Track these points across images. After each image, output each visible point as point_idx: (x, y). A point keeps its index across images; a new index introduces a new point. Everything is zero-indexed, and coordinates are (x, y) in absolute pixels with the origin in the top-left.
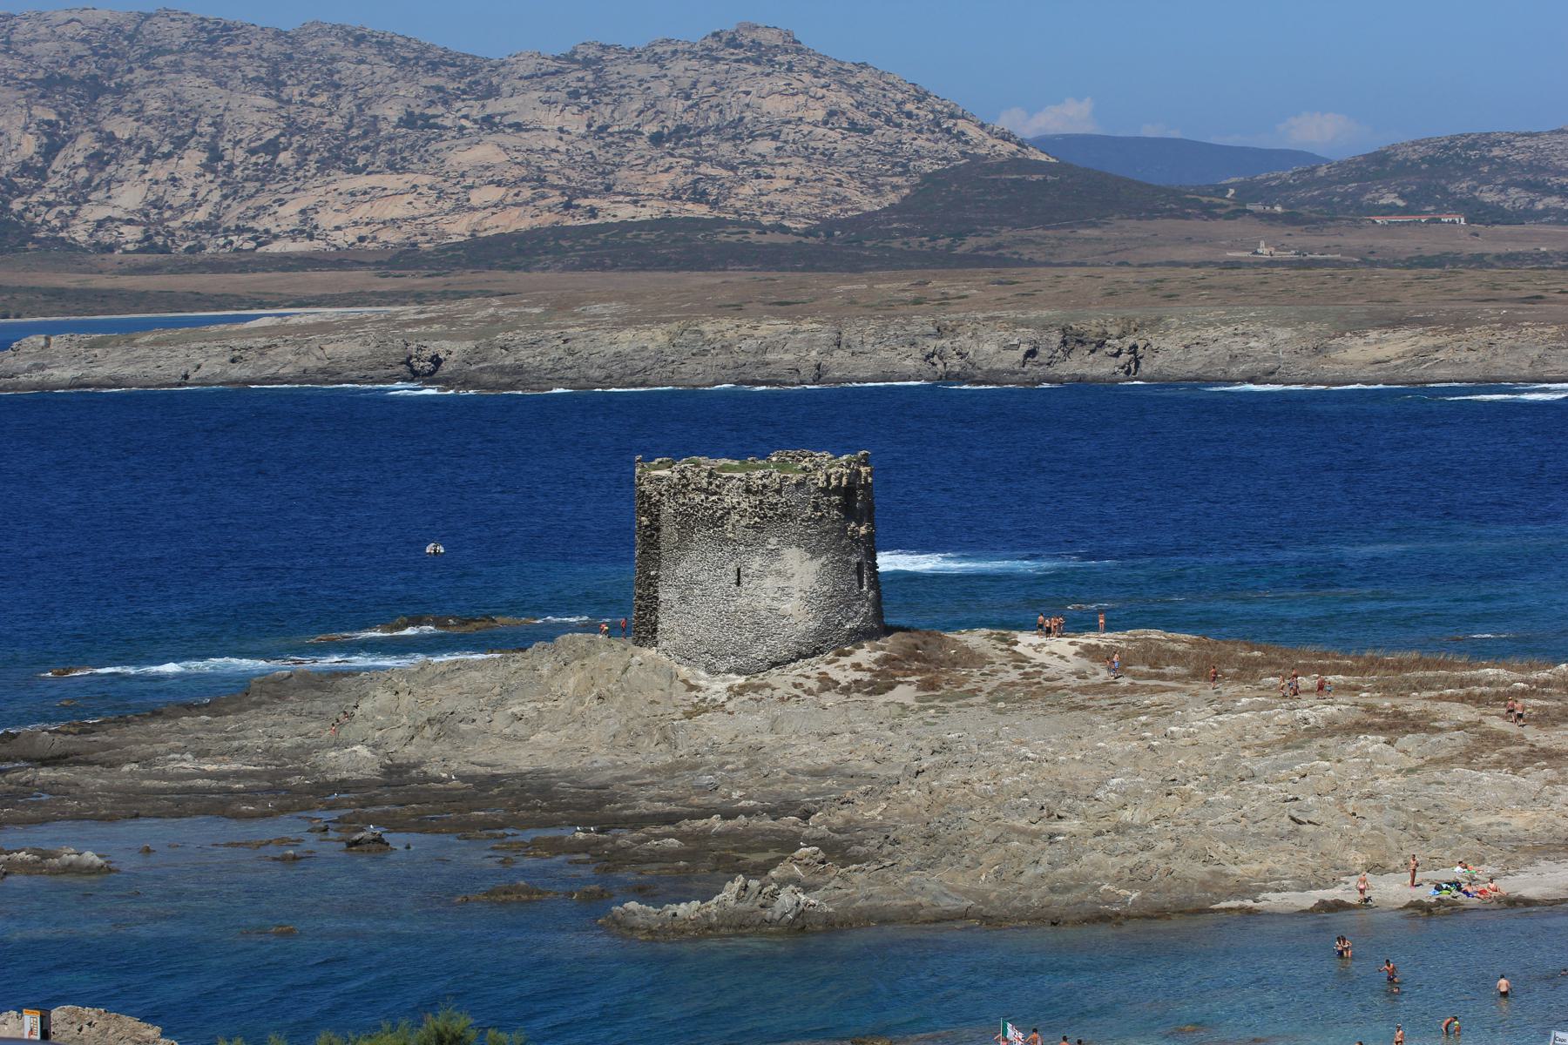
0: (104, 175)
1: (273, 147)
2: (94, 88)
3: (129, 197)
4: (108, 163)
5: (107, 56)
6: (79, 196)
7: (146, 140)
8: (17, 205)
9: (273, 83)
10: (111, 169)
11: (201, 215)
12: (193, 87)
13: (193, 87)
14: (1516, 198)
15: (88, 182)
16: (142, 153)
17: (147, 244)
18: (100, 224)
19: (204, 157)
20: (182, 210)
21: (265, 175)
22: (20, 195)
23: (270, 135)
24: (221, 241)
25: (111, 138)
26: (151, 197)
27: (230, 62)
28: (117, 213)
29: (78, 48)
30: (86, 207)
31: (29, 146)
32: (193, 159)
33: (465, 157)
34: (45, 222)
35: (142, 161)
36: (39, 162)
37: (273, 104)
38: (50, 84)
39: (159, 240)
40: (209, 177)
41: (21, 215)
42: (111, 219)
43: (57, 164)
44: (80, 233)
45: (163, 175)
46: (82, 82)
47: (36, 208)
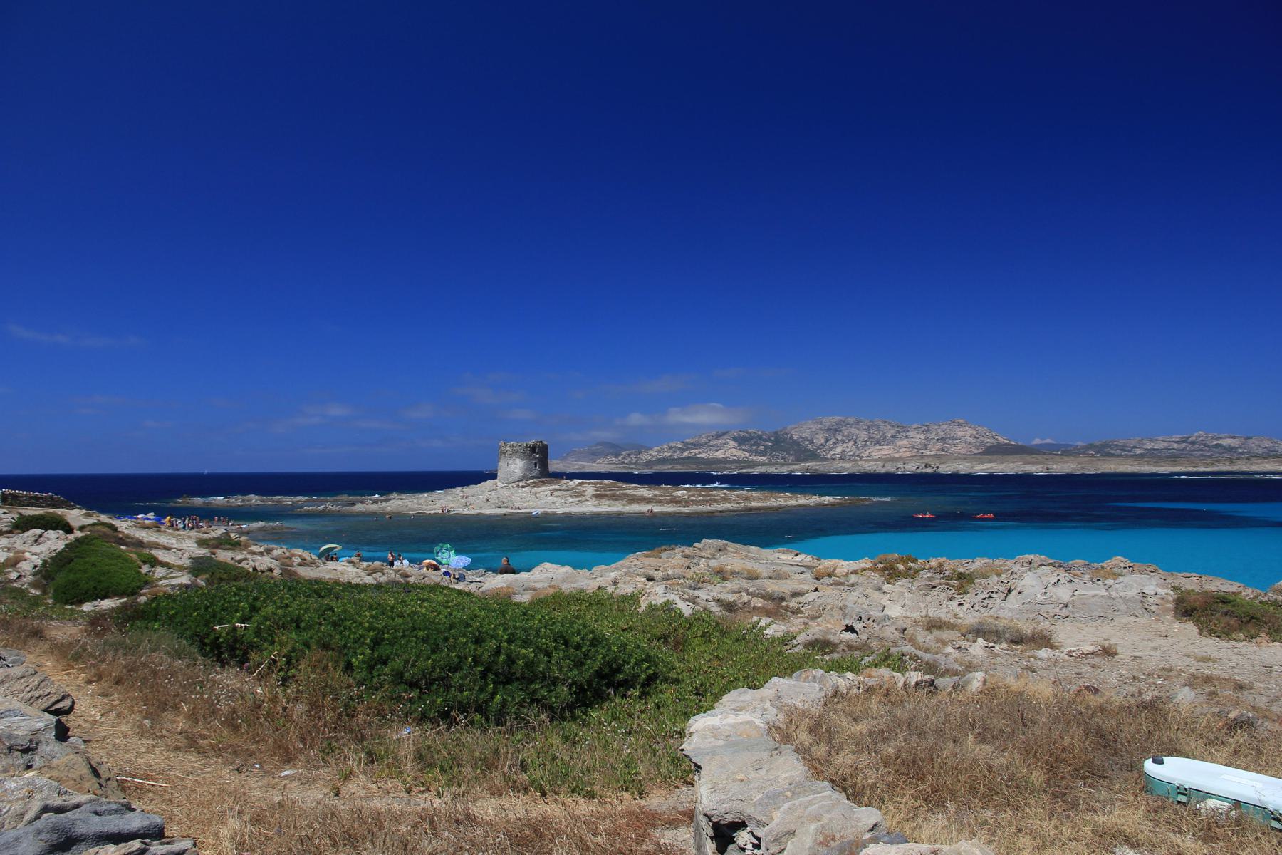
2: (836, 430)
3: (839, 450)
6: (830, 450)
9: (868, 430)
12: (853, 430)
13: (853, 430)
14: (1119, 452)
21: (864, 446)
33: (900, 443)
38: (828, 430)
47: (822, 452)
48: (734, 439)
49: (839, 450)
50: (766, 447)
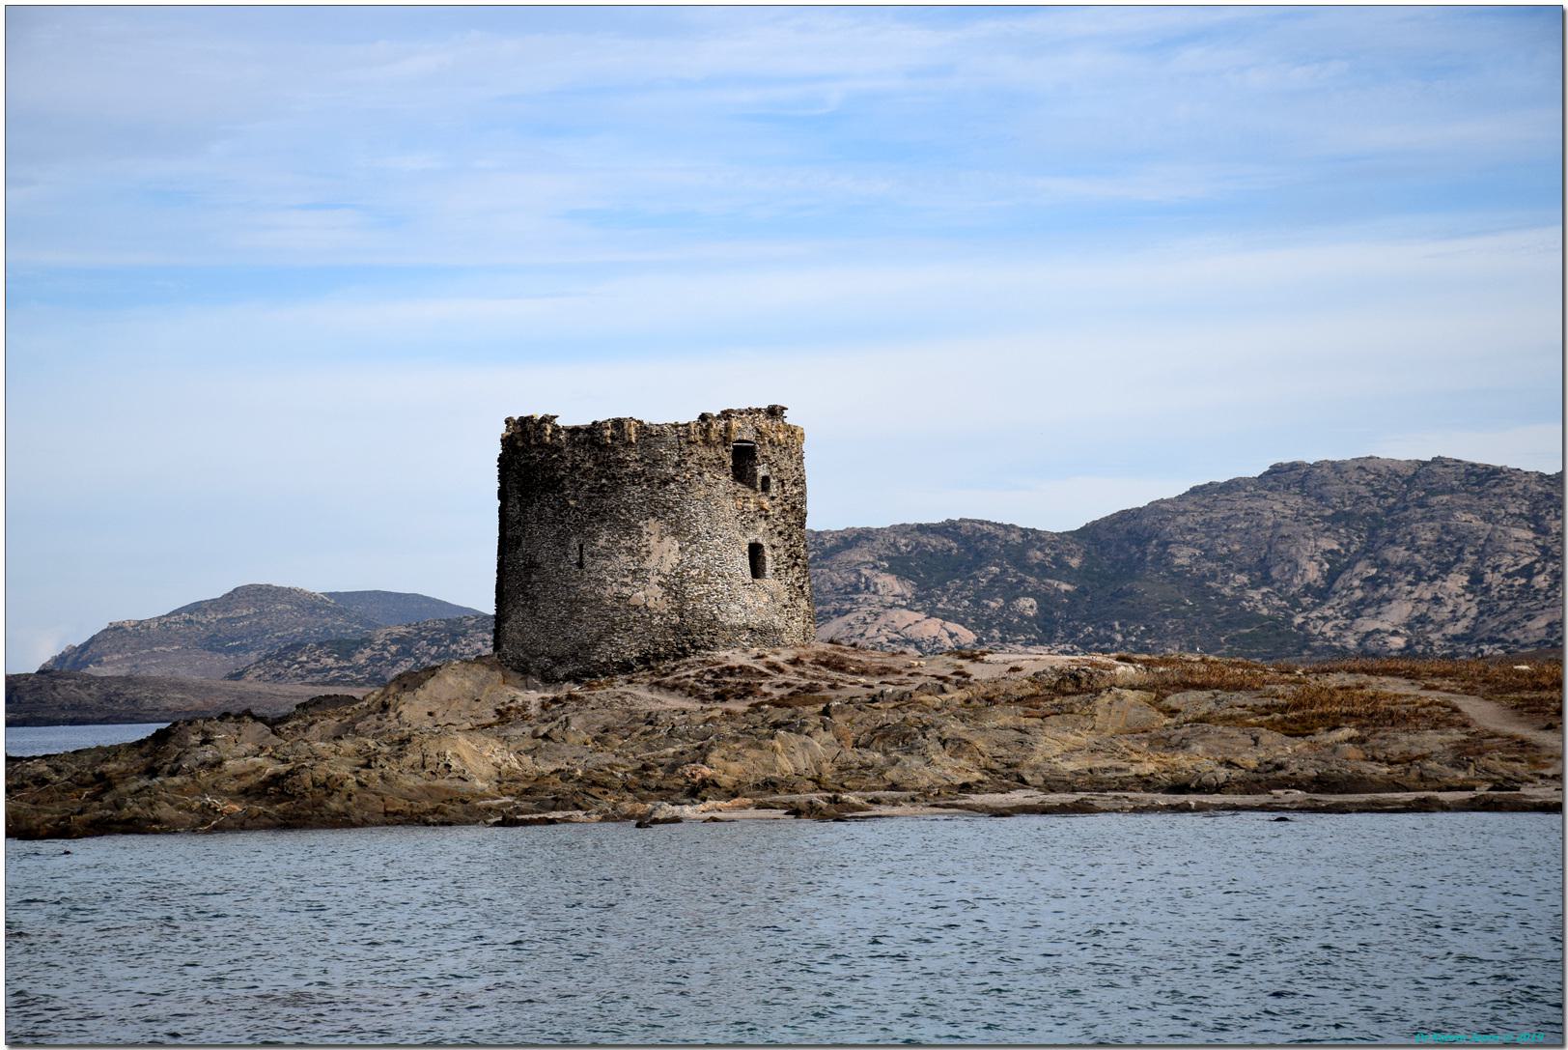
0: (1377, 595)
1: (1528, 572)
2: (1374, 524)
3: (1398, 612)
4: (1379, 585)
5: (1385, 497)
6: (1356, 610)
7: (1416, 567)
8: (1298, 620)
10: (1385, 590)
11: (1459, 628)
15: (1362, 601)
16: (1410, 578)
17: (1408, 651)
18: (1369, 634)
19: (1464, 580)
20: (1442, 625)
22: (1304, 610)
23: (1527, 561)
24: (1473, 650)
25: (1385, 564)
26: (1416, 614)
27: (1496, 501)
28: (1386, 626)
29: (1363, 490)
30: (1359, 621)
31: (1313, 573)
32: (1456, 582)
34: (1321, 633)
35: (1410, 583)
36: (1321, 584)
37: (1530, 535)
39: (1419, 648)
40: (1469, 596)
41: (1300, 627)
42: (1378, 631)
43: (1338, 585)
44: (1351, 642)
45: (1428, 595)
46: (1362, 518)
48: (899, 566)
49: (1398, 612)
50: (1046, 601)
